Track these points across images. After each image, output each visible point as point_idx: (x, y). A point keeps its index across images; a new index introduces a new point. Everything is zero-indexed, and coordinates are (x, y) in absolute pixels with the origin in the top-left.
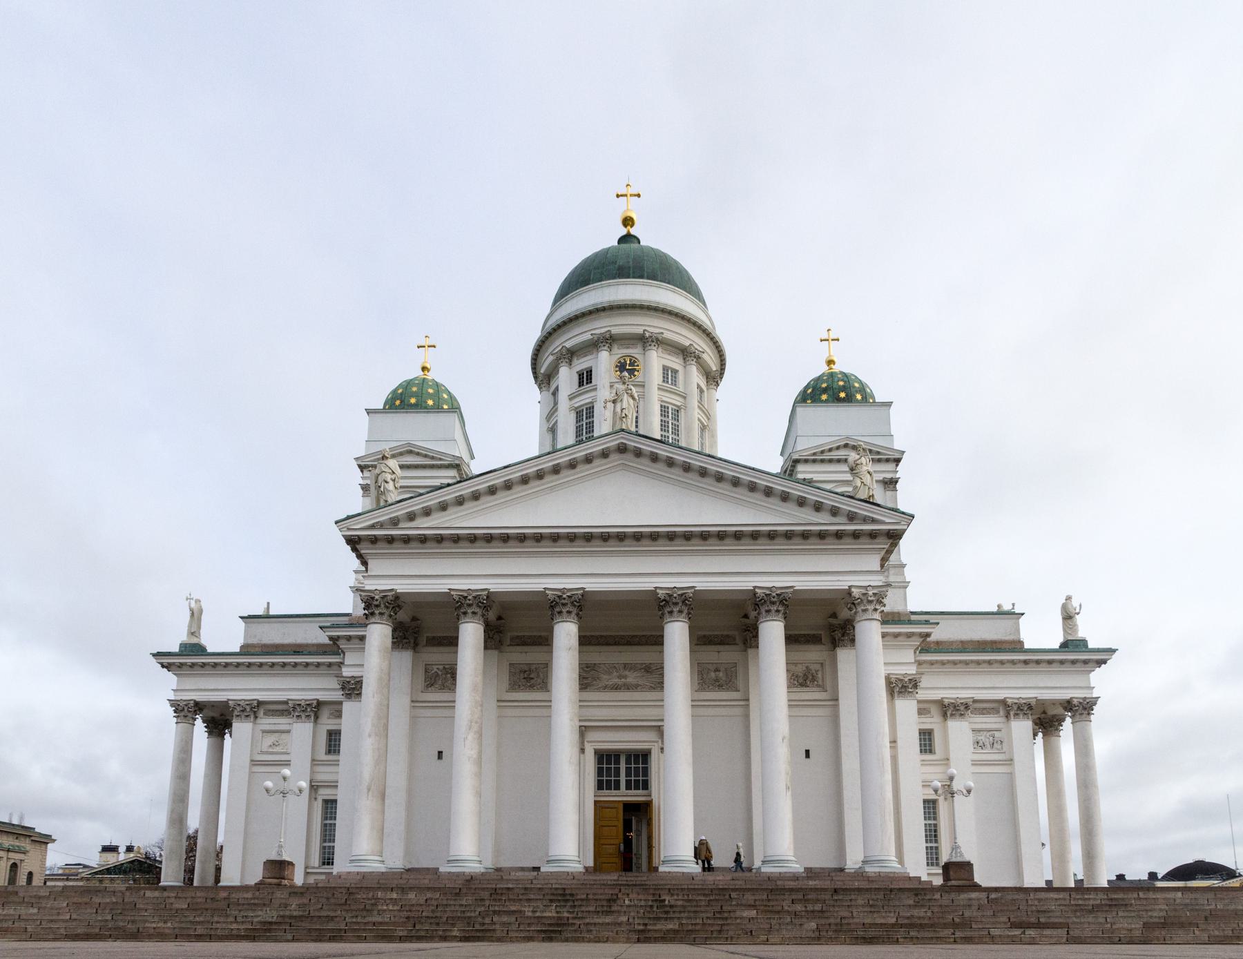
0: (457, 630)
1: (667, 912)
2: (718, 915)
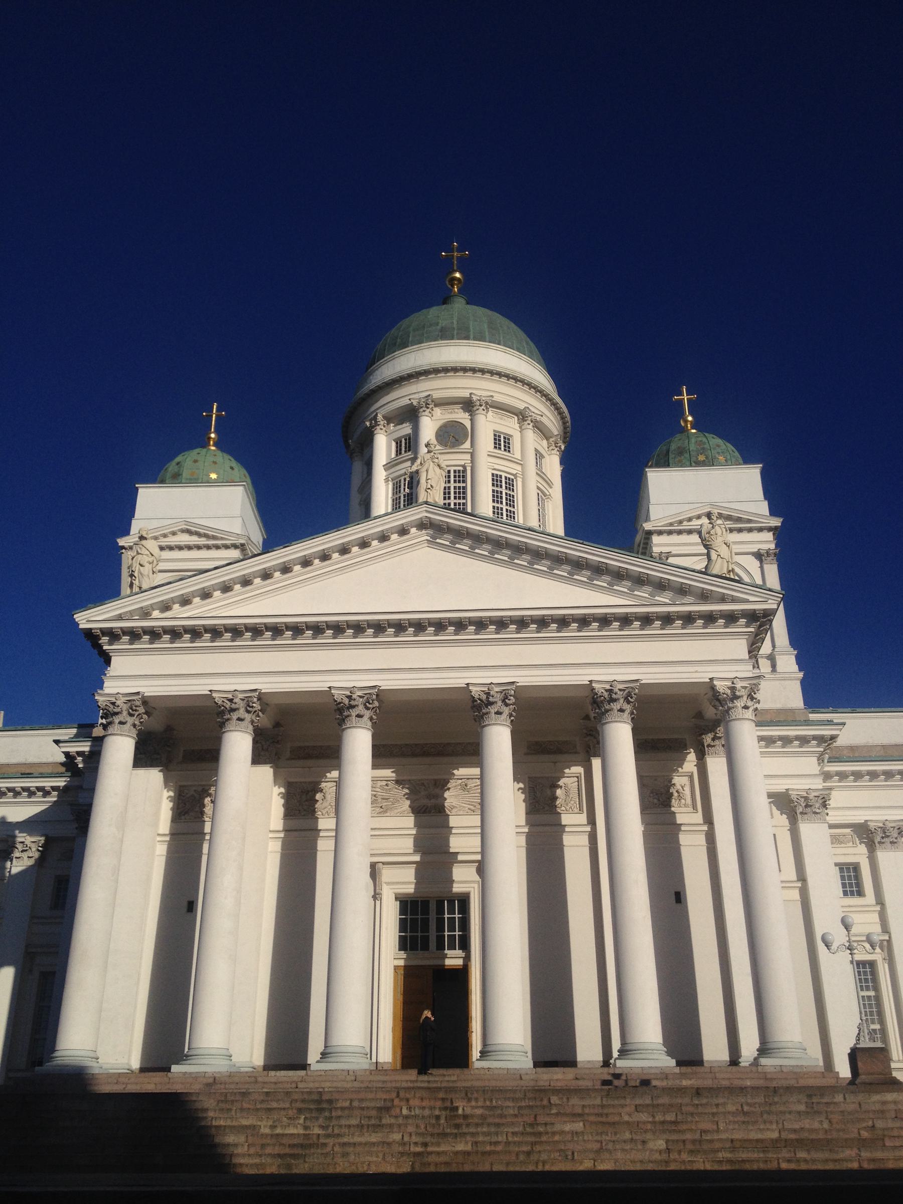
1: (457, 1126)
2: (528, 1130)
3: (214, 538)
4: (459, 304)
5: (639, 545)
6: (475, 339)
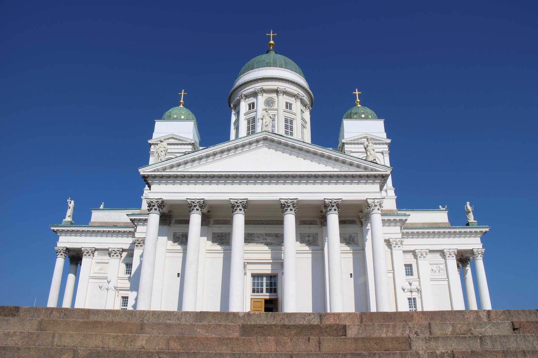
0: (189, 217)
3: (182, 140)
4: (273, 54)
5: (340, 148)
6: (279, 67)
